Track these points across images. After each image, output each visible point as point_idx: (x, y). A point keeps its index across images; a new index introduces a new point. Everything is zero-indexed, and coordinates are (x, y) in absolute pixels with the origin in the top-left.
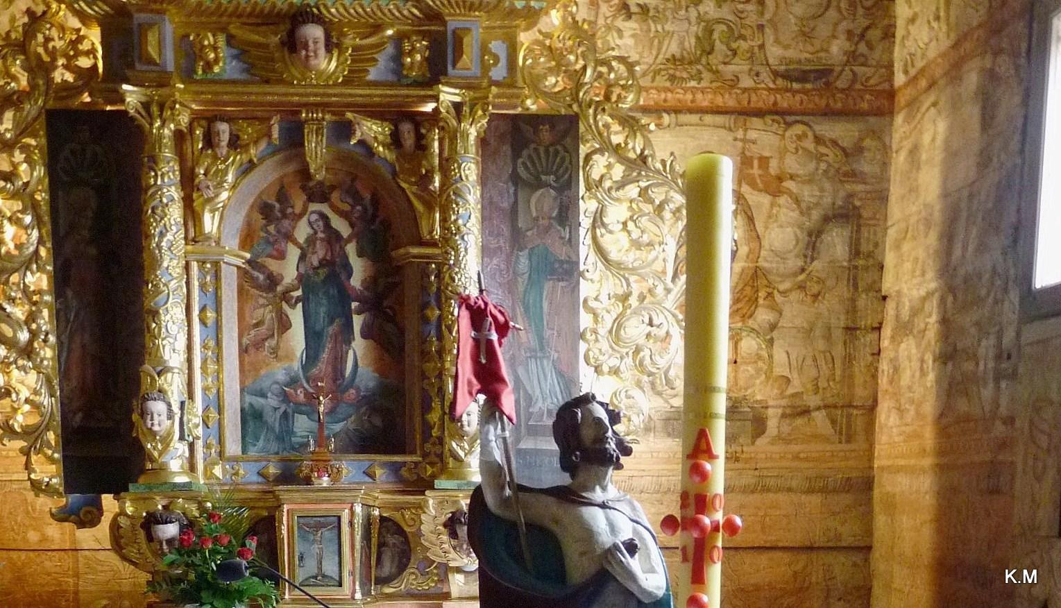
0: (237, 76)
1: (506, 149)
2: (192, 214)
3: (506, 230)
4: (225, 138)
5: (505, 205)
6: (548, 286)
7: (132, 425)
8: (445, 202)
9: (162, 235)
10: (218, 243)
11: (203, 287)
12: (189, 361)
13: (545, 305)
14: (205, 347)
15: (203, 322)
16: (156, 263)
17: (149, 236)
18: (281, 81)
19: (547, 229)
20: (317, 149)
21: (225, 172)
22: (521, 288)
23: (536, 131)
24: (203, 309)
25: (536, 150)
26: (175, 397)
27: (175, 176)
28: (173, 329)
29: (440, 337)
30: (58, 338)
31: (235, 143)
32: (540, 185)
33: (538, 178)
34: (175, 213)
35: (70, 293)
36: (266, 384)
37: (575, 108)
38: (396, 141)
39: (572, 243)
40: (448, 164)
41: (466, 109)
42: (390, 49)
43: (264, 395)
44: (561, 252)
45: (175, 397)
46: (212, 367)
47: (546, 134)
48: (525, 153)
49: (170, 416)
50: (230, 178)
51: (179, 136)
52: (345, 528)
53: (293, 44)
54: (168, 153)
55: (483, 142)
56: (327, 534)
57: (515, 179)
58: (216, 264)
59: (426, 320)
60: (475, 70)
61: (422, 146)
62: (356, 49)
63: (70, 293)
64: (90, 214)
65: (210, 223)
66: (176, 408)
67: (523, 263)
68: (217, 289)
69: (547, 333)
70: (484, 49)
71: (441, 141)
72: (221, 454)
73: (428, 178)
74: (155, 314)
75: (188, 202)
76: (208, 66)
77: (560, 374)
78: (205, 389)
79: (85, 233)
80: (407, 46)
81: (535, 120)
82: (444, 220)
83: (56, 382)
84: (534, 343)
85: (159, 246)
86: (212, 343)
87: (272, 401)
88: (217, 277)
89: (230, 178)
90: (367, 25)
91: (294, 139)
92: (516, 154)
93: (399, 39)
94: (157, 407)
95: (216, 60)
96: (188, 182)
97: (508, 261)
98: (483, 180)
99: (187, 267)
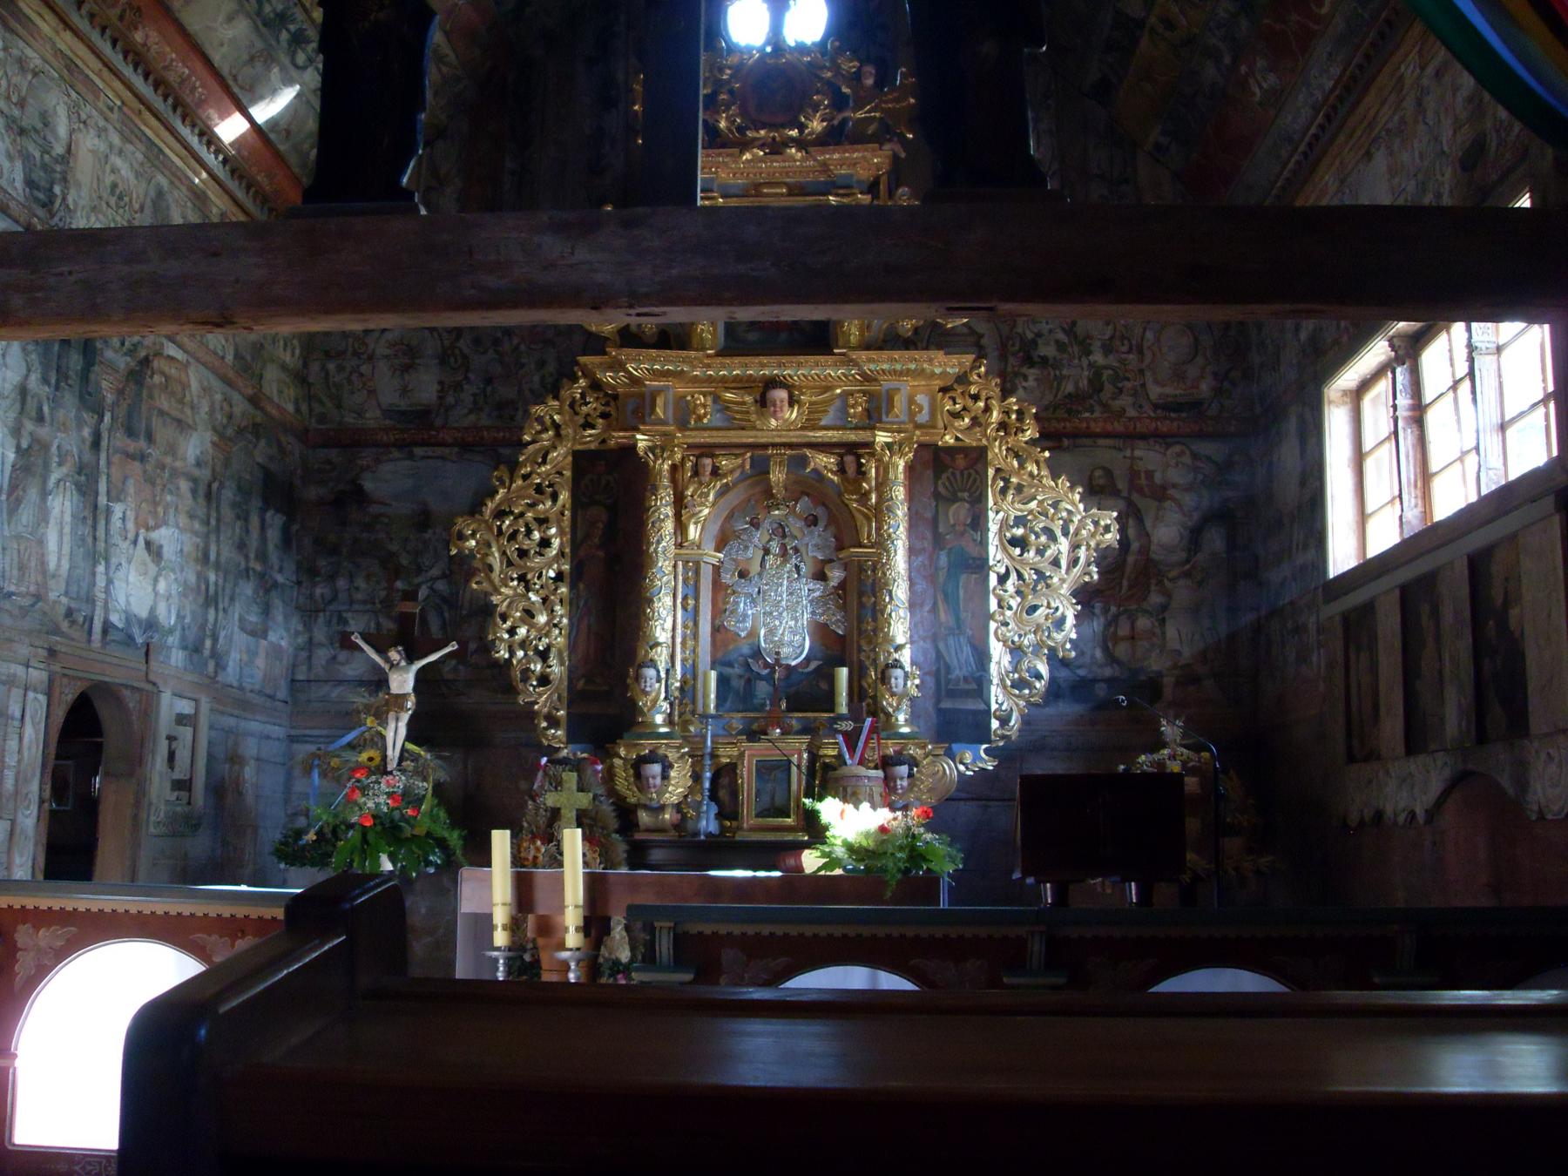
0: (720, 424)
1: (929, 473)
2: (681, 527)
3: (929, 535)
4: (709, 469)
5: (929, 515)
6: (963, 578)
7: (626, 687)
8: (880, 513)
9: (658, 542)
10: (699, 547)
11: (685, 581)
12: (673, 637)
13: (961, 592)
14: (685, 626)
15: (684, 608)
16: (653, 563)
17: (649, 544)
18: (754, 428)
19: (962, 534)
20: (777, 476)
21: (707, 495)
22: (941, 580)
23: (953, 460)
24: (685, 598)
25: (953, 474)
26: (662, 667)
27: (669, 499)
28: (664, 613)
29: (875, 619)
30: (570, 620)
31: (715, 472)
32: (955, 499)
33: (954, 494)
34: (669, 526)
35: (581, 586)
36: (733, 656)
37: (984, 442)
38: (842, 470)
39: (984, 544)
40: (883, 484)
41: (896, 447)
42: (838, 403)
43: (730, 664)
44: (974, 551)
45: (662, 667)
46: (690, 643)
47: (961, 461)
48: (944, 476)
49: (659, 680)
50: (711, 498)
51: (674, 468)
52: (794, 769)
53: (763, 402)
54: (666, 482)
55: (910, 468)
56: (779, 774)
57: (937, 495)
58: (697, 564)
59: (861, 605)
60: (903, 418)
61: (861, 473)
62: (811, 403)
63: (581, 586)
64: (601, 525)
65: (693, 532)
66: (663, 675)
67: (943, 560)
68: (697, 582)
69: (963, 615)
70: (911, 401)
71: (877, 469)
72: (693, 713)
73: (866, 495)
74: (650, 602)
75: (678, 516)
76: (700, 418)
77: (974, 648)
78: (684, 660)
79: (596, 540)
80: (851, 401)
81: (950, 450)
82: (879, 529)
83: (565, 654)
84: (952, 623)
85: (656, 551)
86: (691, 624)
87: (737, 670)
88: (697, 572)
89: (711, 498)
90: (820, 387)
91: (761, 469)
92: (937, 477)
93: (846, 394)
94: (650, 673)
95: (705, 415)
96: (679, 503)
97: (931, 559)
98: (911, 497)
99: (675, 566)
